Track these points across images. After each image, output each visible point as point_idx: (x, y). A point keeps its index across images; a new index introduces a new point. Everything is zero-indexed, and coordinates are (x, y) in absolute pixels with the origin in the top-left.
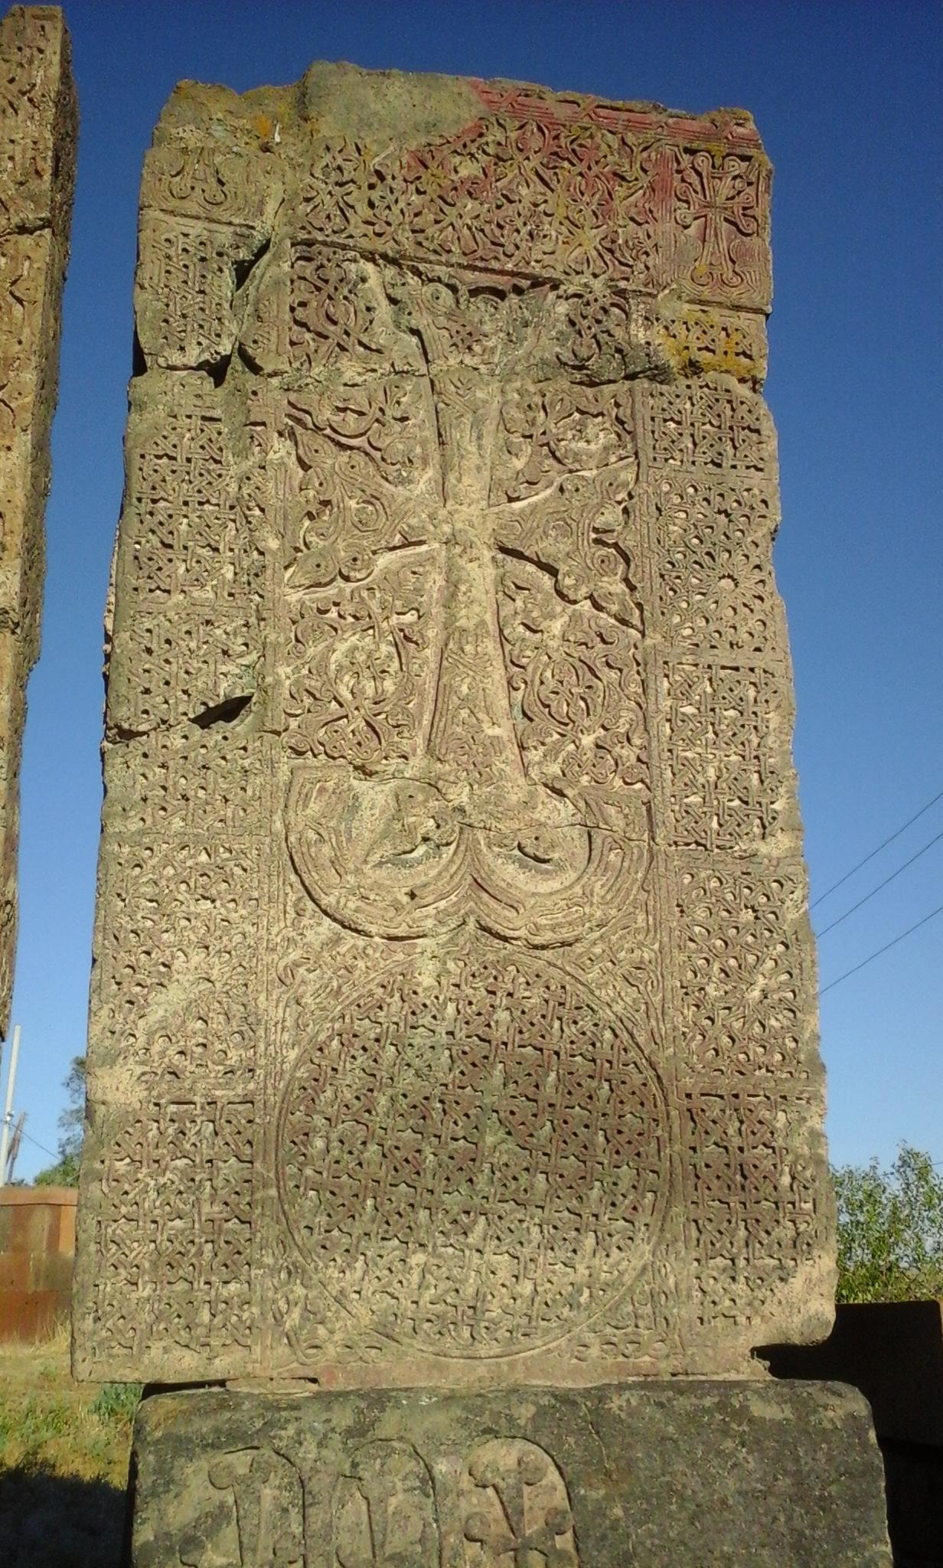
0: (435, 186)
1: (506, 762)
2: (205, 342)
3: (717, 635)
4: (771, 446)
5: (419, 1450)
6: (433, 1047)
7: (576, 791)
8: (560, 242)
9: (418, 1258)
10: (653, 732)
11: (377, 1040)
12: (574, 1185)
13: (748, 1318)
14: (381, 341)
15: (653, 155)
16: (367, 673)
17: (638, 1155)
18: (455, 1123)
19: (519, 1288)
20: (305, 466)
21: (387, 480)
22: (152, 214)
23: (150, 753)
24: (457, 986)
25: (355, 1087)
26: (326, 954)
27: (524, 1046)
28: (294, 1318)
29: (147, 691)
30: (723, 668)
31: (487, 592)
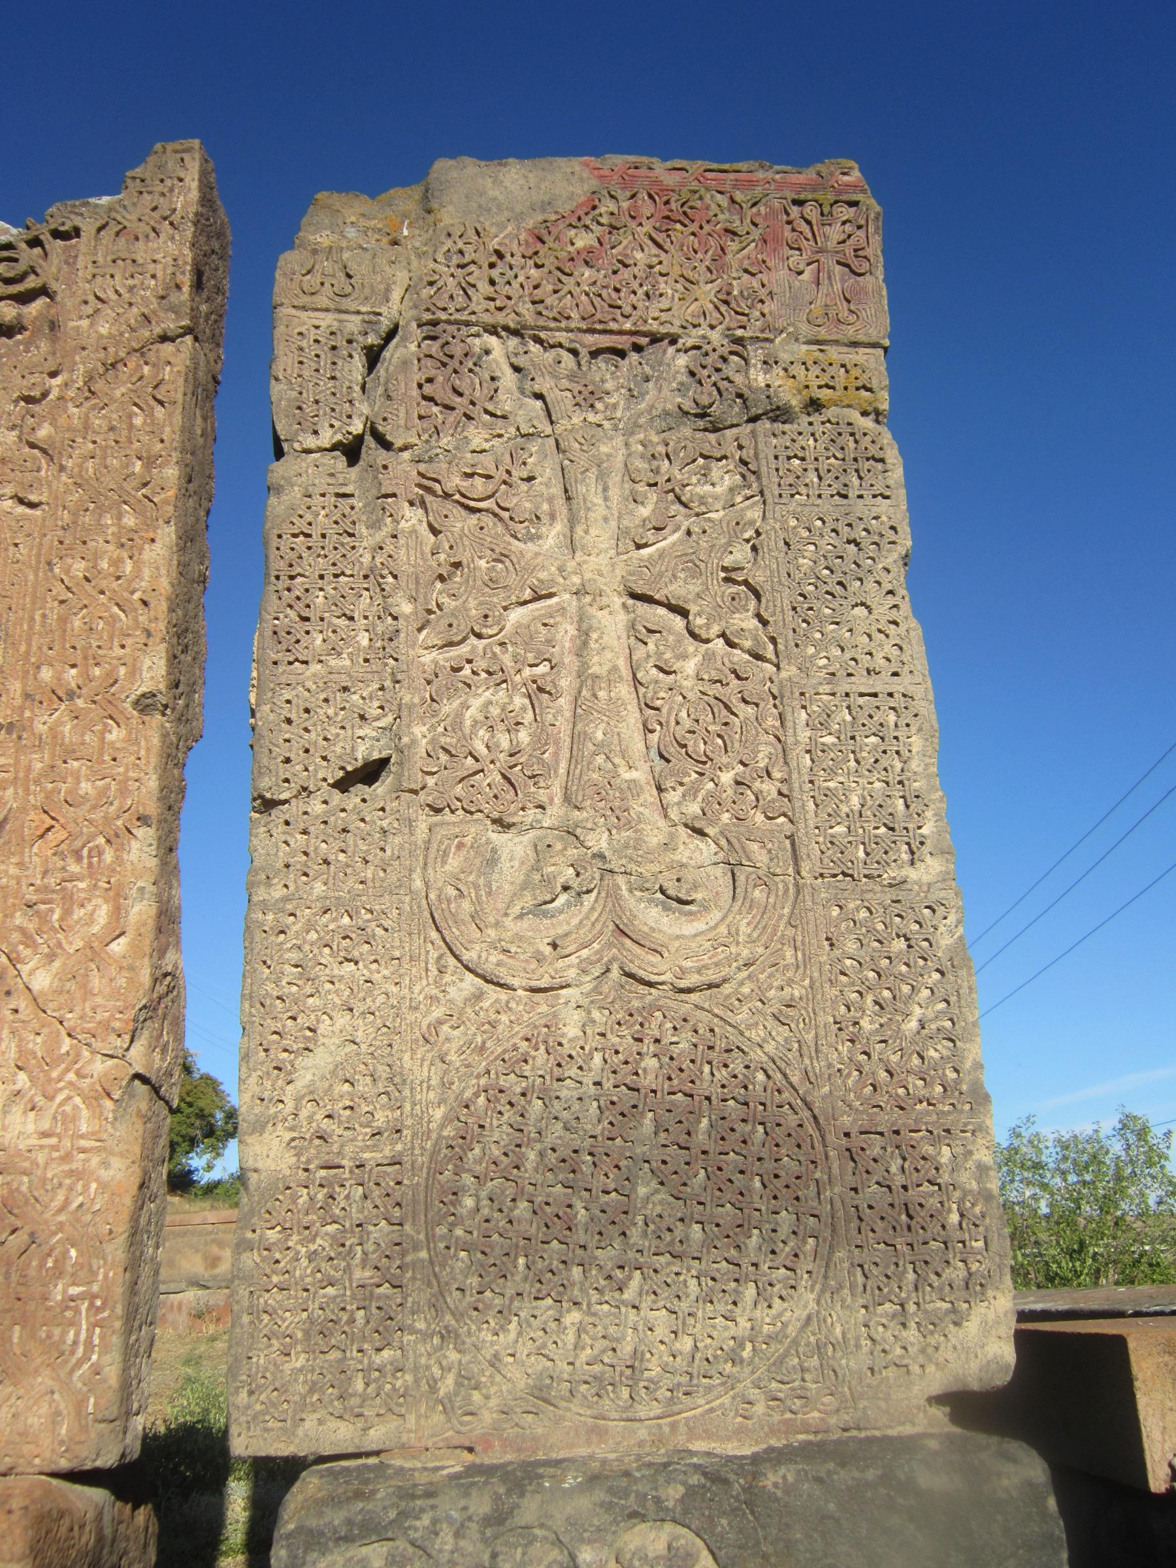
0: (552, 259)
1: (644, 805)
3: (853, 663)
4: (897, 474)
5: (561, 1537)
6: (580, 1099)
7: (717, 830)
8: (676, 299)
9: (573, 1317)
10: (793, 764)
11: (524, 1095)
12: (731, 1234)
13: (922, 1366)
14: (506, 408)
15: (762, 209)
16: (501, 727)
17: (797, 1199)
18: (606, 1175)
19: (678, 1345)
20: (435, 532)
21: (516, 538)
22: (285, 311)
23: (291, 820)
24: (603, 1035)
25: (502, 1143)
26: (469, 1010)
27: (674, 1093)
28: (448, 1384)
29: (288, 760)
30: (862, 695)
31: (619, 638)
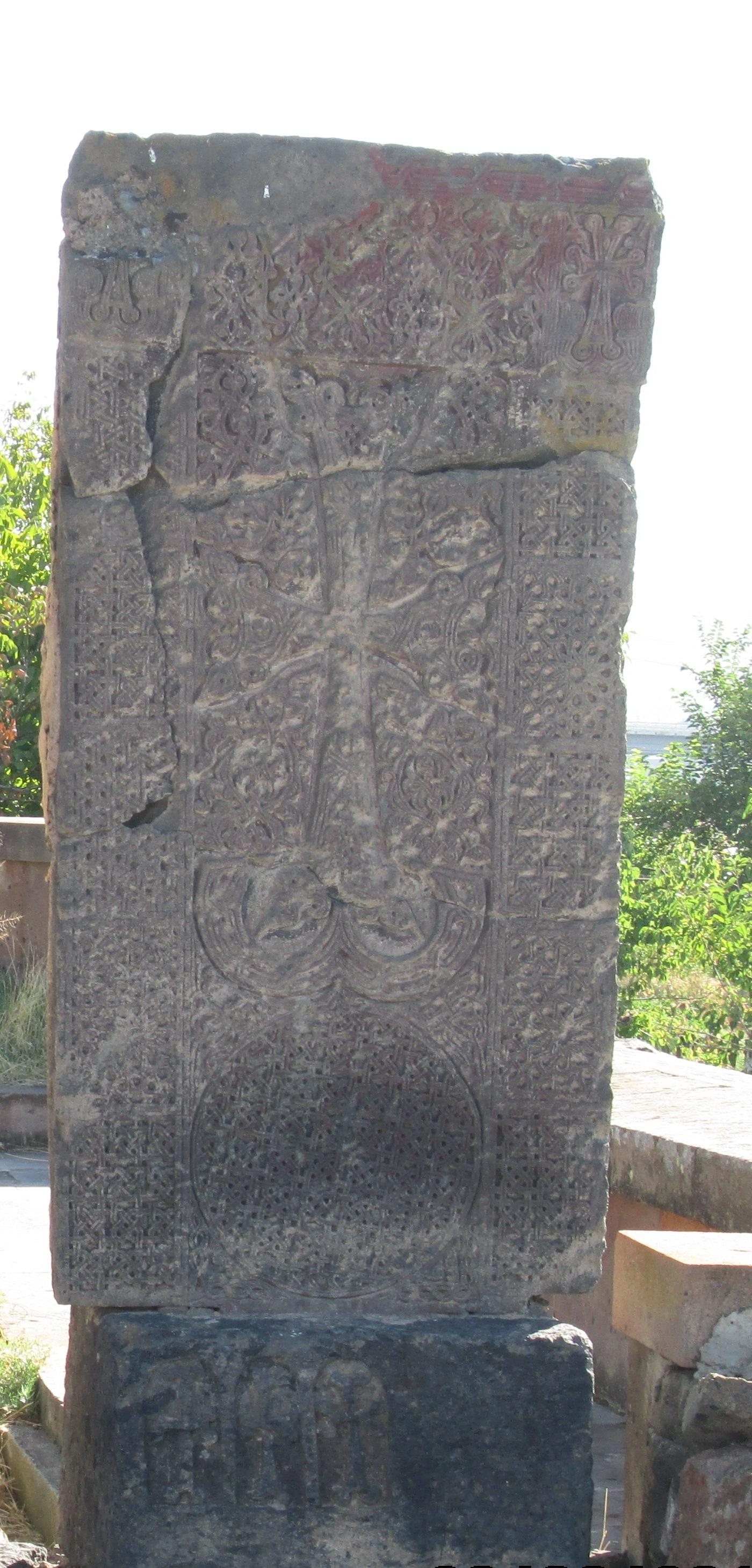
2: (125, 470)
9: (290, 1231)
11: (264, 1076)
18: (320, 1137)
